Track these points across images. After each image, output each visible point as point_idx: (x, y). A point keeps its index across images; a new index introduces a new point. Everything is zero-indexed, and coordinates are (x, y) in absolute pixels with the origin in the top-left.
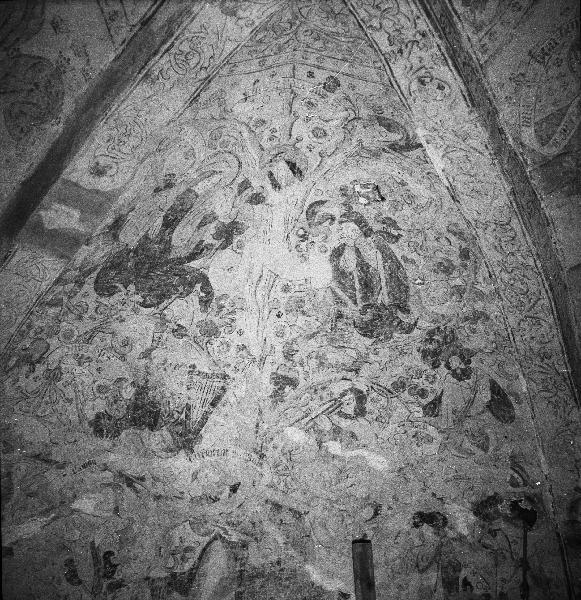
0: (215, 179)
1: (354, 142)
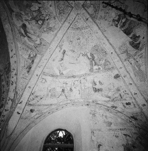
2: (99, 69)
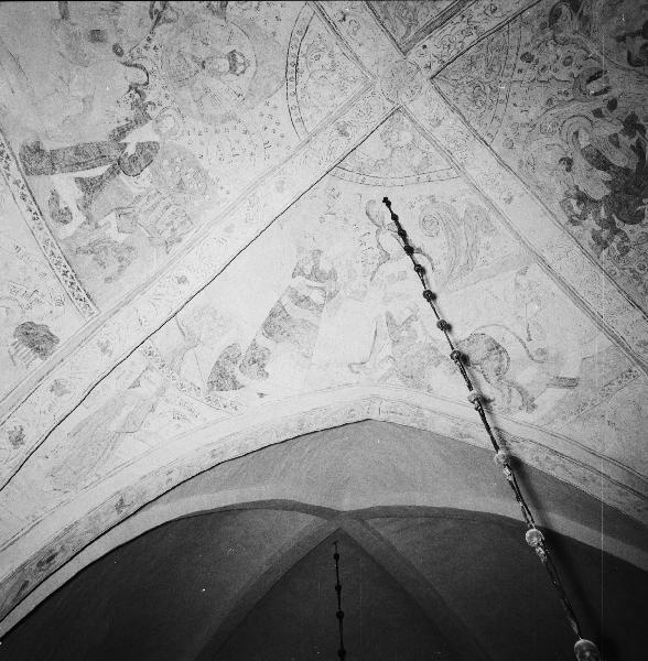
0: (582, 133)
1: (576, 36)
2: (63, 217)
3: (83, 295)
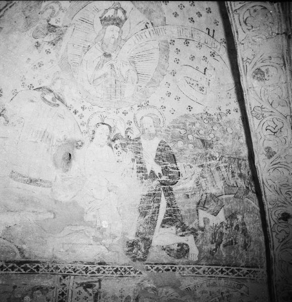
3: (245, 270)
